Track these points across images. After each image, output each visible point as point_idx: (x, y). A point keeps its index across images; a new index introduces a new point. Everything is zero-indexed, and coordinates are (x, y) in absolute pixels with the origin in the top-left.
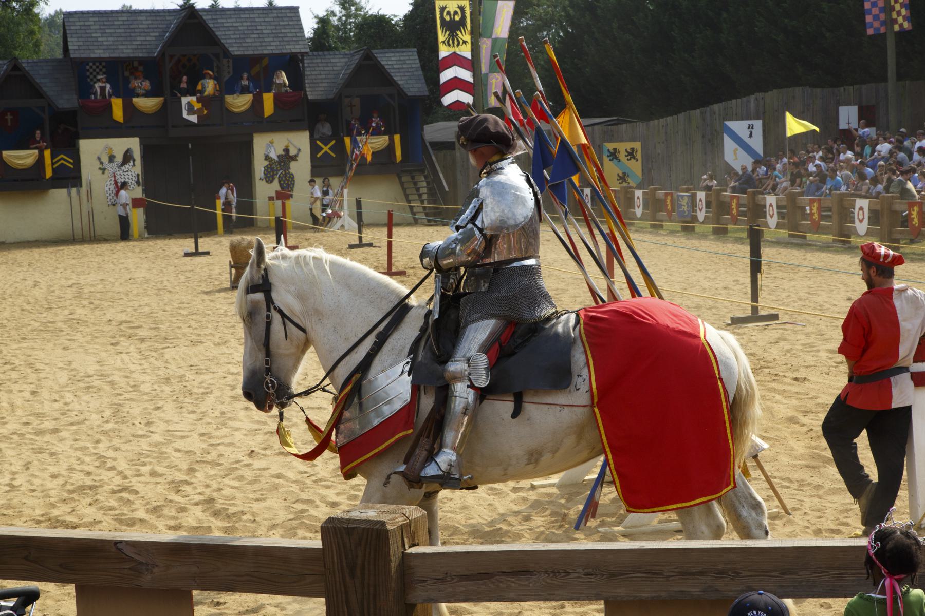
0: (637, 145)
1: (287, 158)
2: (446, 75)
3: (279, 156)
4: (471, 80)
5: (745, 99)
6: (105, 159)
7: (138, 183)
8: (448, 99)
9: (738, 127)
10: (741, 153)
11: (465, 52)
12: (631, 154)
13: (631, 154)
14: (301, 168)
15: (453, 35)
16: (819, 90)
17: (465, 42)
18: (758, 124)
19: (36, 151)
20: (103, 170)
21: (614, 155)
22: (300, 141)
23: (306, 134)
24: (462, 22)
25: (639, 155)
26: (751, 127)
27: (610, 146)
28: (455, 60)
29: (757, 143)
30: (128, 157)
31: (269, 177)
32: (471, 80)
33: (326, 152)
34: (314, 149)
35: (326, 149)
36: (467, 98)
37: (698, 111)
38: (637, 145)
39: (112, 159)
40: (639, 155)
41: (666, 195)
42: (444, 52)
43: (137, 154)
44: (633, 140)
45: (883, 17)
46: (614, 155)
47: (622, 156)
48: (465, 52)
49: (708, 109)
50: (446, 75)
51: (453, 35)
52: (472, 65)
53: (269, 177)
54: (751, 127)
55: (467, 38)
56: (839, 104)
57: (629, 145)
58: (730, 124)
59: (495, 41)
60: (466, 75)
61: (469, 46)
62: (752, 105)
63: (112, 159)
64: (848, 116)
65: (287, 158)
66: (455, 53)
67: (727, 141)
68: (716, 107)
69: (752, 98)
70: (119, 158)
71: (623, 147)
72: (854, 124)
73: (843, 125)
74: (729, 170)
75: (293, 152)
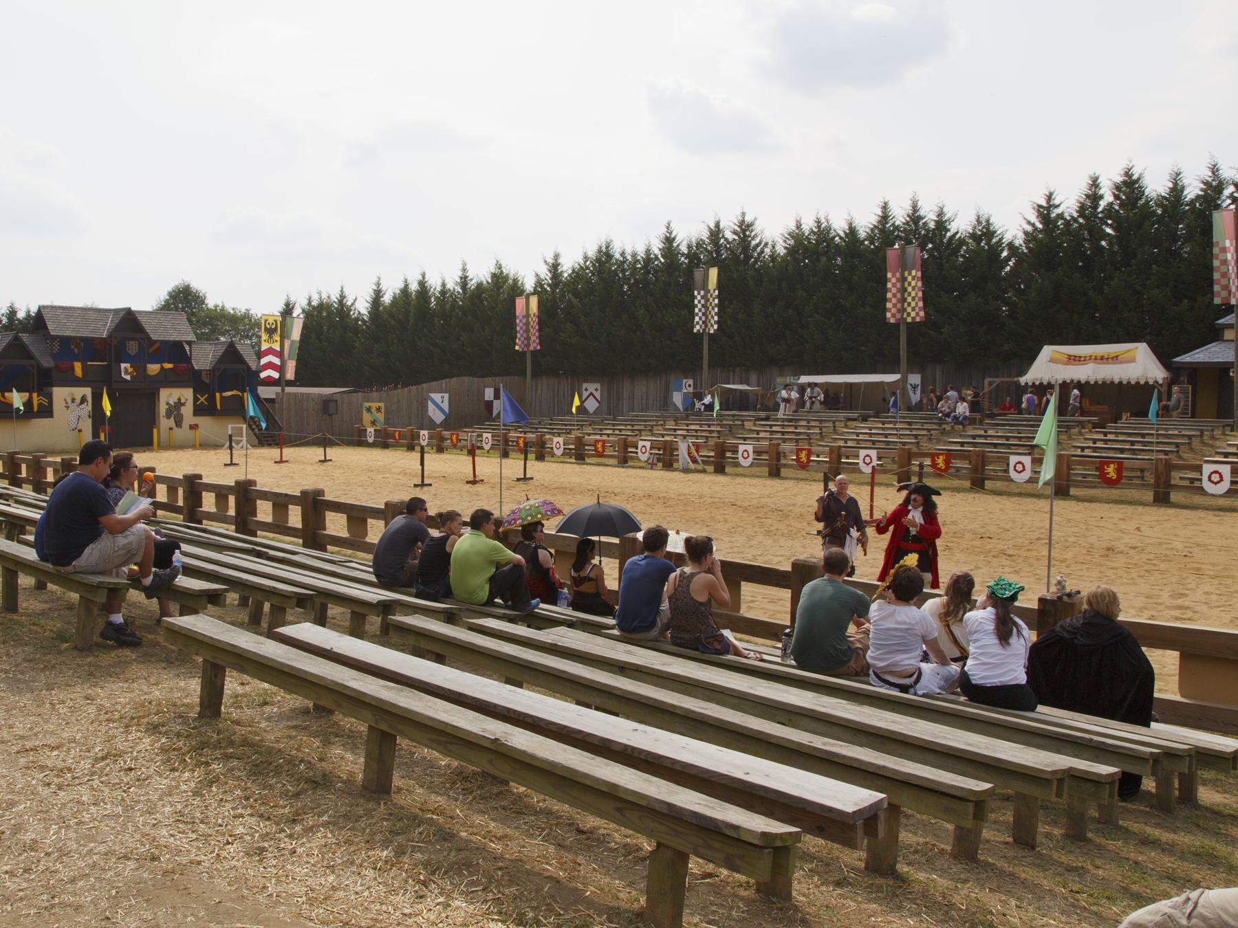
0: (382, 405)
1: (179, 404)
2: (264, 361)
3: (175, 403)
4: (279, 364)
5: (440, 382)
6: (69, 401)
7: (89, 416)
8: (263, 375)
9: (436, 397)
10: (438, 411)
11: (277, 347)
12: (379, 409)
13: (379, 409)
14: (187, 410)
15: (270, 337)
16: (476, 379)
17: (276, 341)
18: (446, 396)
19: (28, 394)
20: (68, 407)
21: (369, 410)
22: (187, 394)
23: (191, 390)
24: (275, 330)
25: (383, 410)
26: (443, 397)
27: (367, 405)
28: (270, 351)
29: (446, 406)
30: (83, 400)
31: (168, 416)
32: (279, 364)
33: (202, 402)
34: (196, 399)
35: (202, 399)
36: (276, 375)
37: (414, 387)
38: (382, 405)
39: (73, 400)
40: (383, 410)
41: (452, 434)
42: (265, 346)
43: (89, 399)
44: (380, 401)
45: (526, 342)
46: (369, 410)
47: (374, 410)
48: (277, 347)
49: (420, 386)
50: (264, 361)
51: (270, 337)
52: (280, 354)
53: (168, 416)
54: (443, 397)
55: (278, 338)
56: (485, 387)
57: (378, 404)
58: (432, 395)
59: (293, 341)
60: (277, 361)
61: (279, 343)
62: (444, 385)
63: (73, 400)
64: (489, 394)
65: (179, 404)
66: (271, 348)
67: (430, 404)
68: (424, 385)
69: (444, 381)
70: (78, 400)
71: (374, 405)
72: (492, 398)
73: (487, 398)
74: (431, 420)
75: (183, 401)
